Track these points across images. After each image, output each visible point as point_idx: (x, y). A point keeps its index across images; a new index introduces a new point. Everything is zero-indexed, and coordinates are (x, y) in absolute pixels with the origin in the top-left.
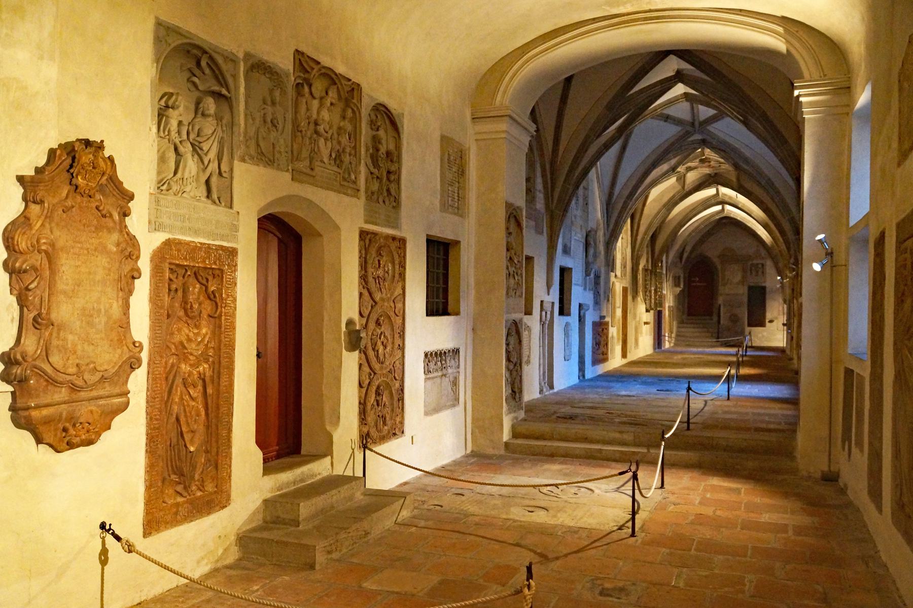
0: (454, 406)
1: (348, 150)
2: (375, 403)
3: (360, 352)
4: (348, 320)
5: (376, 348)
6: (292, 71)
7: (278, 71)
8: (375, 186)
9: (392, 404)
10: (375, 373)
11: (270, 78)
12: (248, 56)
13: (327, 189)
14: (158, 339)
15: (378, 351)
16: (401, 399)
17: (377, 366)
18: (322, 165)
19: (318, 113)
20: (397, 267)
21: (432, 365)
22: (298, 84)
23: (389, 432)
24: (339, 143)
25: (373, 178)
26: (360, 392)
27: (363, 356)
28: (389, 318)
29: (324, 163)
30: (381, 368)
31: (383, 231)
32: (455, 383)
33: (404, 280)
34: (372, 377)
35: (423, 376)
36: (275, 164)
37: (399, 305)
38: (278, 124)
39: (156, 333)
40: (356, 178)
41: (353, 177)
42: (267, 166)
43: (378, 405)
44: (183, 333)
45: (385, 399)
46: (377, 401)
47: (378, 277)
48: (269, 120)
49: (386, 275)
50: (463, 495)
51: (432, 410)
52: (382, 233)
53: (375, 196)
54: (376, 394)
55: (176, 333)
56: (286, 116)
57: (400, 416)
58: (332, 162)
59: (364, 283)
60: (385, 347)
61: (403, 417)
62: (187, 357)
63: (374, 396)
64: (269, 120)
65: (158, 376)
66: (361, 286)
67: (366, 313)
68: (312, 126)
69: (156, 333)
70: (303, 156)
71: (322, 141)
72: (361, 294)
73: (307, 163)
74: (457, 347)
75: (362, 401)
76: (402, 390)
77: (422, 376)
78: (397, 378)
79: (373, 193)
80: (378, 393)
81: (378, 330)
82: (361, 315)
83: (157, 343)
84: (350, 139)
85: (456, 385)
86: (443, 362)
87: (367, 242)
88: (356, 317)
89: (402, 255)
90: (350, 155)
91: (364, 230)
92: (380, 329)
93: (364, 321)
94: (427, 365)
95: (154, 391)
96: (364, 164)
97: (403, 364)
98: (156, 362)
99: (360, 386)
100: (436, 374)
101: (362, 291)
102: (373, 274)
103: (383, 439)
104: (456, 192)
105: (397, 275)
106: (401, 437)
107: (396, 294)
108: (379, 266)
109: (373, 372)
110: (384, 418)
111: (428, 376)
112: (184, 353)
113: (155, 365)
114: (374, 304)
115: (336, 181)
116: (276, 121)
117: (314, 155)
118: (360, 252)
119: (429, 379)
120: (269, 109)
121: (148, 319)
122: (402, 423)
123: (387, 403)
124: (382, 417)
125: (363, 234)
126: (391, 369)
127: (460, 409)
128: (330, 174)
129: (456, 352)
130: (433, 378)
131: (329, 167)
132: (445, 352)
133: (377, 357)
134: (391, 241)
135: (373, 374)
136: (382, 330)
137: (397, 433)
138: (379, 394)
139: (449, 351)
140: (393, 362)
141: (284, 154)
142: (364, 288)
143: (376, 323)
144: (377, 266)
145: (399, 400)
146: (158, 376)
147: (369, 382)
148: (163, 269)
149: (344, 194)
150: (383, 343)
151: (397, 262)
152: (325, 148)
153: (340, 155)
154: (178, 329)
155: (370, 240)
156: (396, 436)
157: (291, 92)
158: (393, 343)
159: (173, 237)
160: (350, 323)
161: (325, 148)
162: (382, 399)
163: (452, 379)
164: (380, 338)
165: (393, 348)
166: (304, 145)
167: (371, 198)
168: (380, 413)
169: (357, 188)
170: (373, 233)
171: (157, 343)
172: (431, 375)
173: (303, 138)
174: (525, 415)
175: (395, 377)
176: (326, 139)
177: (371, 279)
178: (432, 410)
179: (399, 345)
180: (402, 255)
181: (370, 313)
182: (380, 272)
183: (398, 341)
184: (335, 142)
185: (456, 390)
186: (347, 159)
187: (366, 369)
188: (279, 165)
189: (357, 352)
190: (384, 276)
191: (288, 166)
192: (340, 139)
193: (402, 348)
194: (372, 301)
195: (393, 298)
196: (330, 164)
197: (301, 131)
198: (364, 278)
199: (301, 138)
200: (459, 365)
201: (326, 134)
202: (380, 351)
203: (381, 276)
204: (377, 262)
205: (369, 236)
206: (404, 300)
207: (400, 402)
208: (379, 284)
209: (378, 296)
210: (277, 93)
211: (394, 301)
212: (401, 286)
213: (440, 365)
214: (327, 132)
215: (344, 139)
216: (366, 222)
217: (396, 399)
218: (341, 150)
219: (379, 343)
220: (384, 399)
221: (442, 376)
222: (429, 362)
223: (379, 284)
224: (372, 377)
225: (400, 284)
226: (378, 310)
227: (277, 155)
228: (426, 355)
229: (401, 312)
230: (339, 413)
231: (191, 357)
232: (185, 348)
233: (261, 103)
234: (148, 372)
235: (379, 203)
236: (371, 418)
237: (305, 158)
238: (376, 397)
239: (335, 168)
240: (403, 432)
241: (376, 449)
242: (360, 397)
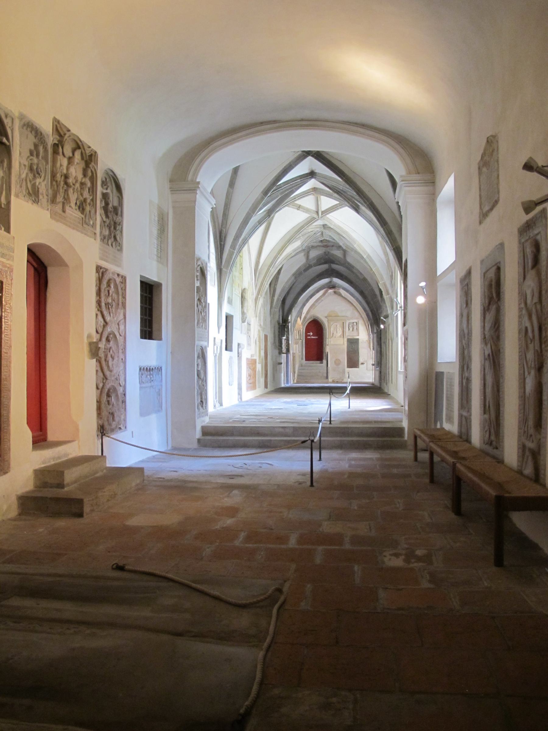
0: (159, 411)
1: (88, 201)
2: (107, 403)
3: (96, 361)
4: (88, 335)
6: (51, 134)
7: (43, 132)
8: (107, 233)
9: (118, 405)
10: (106, 379)
11: (35, 137)
12: (22, 117)
13: (74, 229)
15: (108, 362)
16: (124, 402)
17: (108, 373)
18: (70, 209)
19: (68, 169)
20: (120, 297)
21: (144, 376)
22: (55, 144)
23: (116, 427)
24: (82, 195)
25: (105, 226)
27: (98, 365)
28: (115, 336)
29: (72, 208)
30: (111, 375)
32: (159, 394)
35: (138, 385)
36: (39, 204)
37: (122, 327)
38: (41, 172)
40: (93, 224)
41: (91, 223)
42: (34, 204)
45: (113, 399)
46: (108, 401)
48: (35, 167)
50: (177, 472)
51: (144, 413)
54: (107, 396)
56: (47, 167)
57: (123, 415)
58: (77, 208)
59: (98, 307)
61: (125, 415)
63: (106, 397)
64: (35, 167)
66: (97, 309)
67: (100, 330)
68: (63, 177)
70: (58, 200)
71: (71, 191)
72: (97, 315)
73: (60, 205)
75: (98, 400)
76: (125, 395)
78: (121, 384)
79: (105, 238)
80: (108, 395)
82: (97, 332)
84: (89, 192)
85: (159, 395)
90: (90, 204)
91: (99, 265)
93: (98, 336)
94: (141, 377)
96: (99, 215)
97: (125, 375)
99: (97, 388)
105: (120, 304)
106: (125, 431)
110: (113, 414)
114: (105, 324)
115: (79, 223)
116: (39, 170)
117: (66, 199)
120: (35, 160)
122: (125, 420)
123: (115, 403)
124: (112, 413)
126: (117, 377)
127: (163, 413)
128: (76, 217)
131: (75, 211)
132: (152, 369)
133: (108, 366)
134: (116, 275)
135: (105, 380)
136: (110, 346)
137: (122, 428)
140: (118, 371)
141: (46, 197)
142: (98, 310)
144: (107, 295)
145: (123, 402)
147: (103, 386)
149: (86, 234)
150: (111, 355)
151: (120, 293)
152: (73, 197)
153: (82, 204)
156: (121, 430)
157: (50, 151)
158: (118, 357)
160: (89, 336)
161: (73, 197)
162: (111, 400)
163: (157, 391)
164: (110, 352)
165: (118, 360)
166: (59, 192)
167: (103, 240)
168: (110, 411)
169: (95, 232)
172: (144, 385)
173: (57, 186)
175: (119, 383)
176: (74, 189)
177: (103, 304)
178: (144, 413)
179: (122, 359)
182: (110, 300)
183: (121, 356)
184: (79, 193)
186: (88, 208)
187: (100, 374)
188: (41, 204)
189: (95, 360)
190: (112, 303)
191: (48, 206)
192: (82, 192)
193: (125, 363)
196: (76, 209)
197: (56, 181)
198: (99, 303)
199: (56, 186)
200: (162, 380)
201: (73, 186)
204: (107, 292)
205: (102, 270)
206: (125, 324)
207: (124, 403)
209: (108, 318)
210: (41, 149)
211: (118, 324)
213: (149, 379)
214: (74, 185)
216: (101, 259)
217: (121, 401)
219: (109, 356)
220: (113, 399)
222: (142, 375)
224: (104, 381)
225: (122, 311)
226: (109, 329)
227: (41, 197)
228: (140, 369)
229: (124, 333)
233: (29, 154)
235: (108, 245)
236: (105, 413)
237: (59, 202)
238: (107, 398)
239: (79, 214)
240: (126, 427)
242: (97, 396)
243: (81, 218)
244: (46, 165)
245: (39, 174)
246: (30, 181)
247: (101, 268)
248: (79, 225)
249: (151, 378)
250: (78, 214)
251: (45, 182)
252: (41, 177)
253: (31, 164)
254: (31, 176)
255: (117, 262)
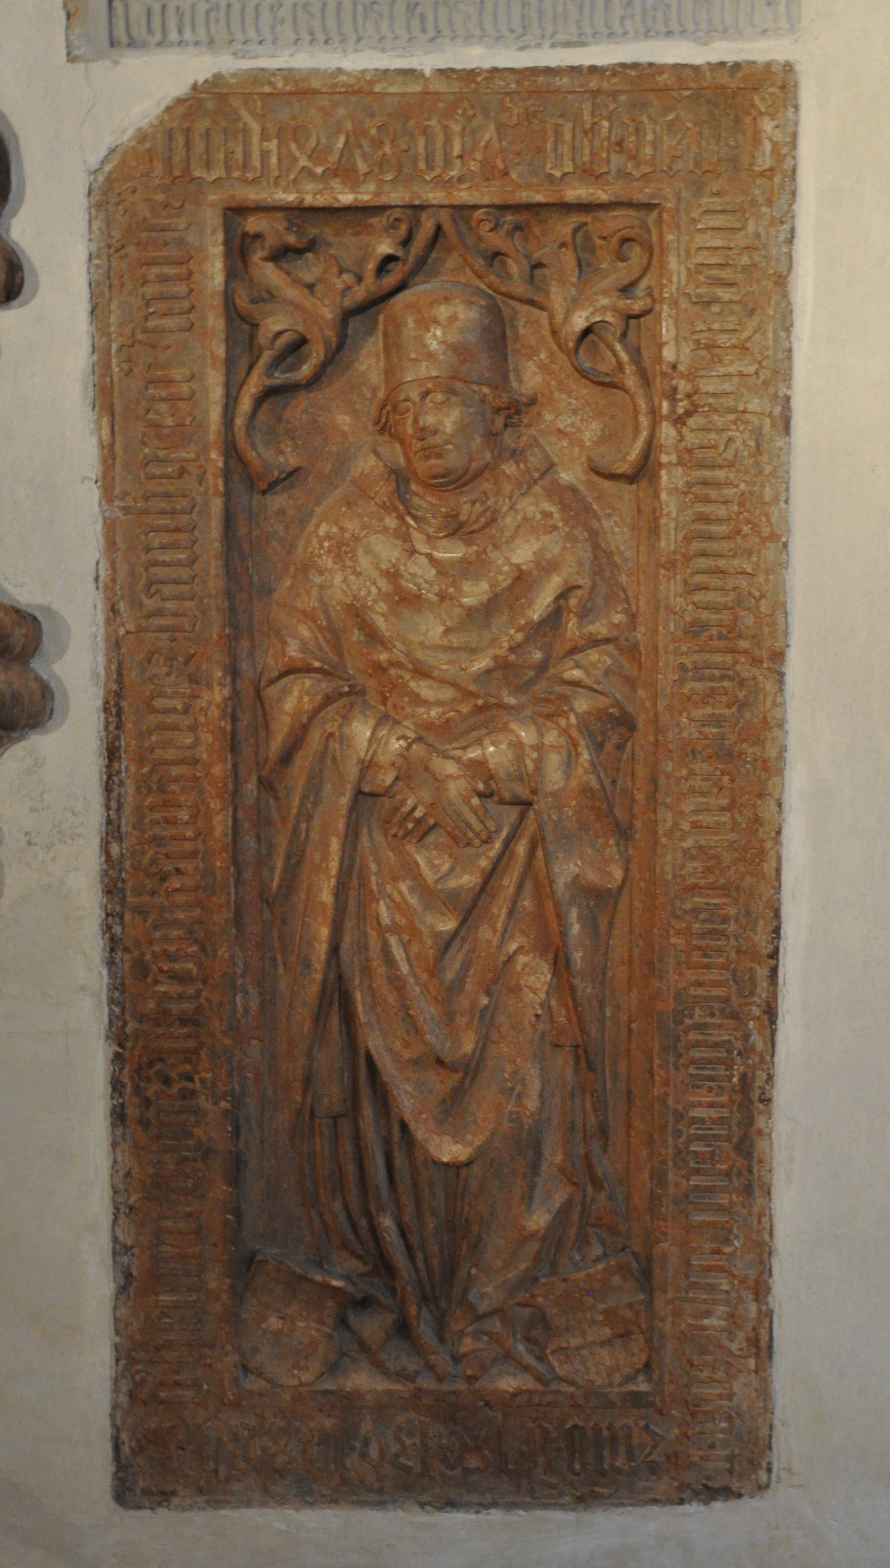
14: (167, 590)
39: (155, 563)
44: (364, 562)
55: (328, 562)
62: (397, 686)
65: (174, 771)
69: (155, 563)
83: (158, 613)
95: (157, 840)
98: (158, 703)
112: (380, 669)
113: (152, 720)
121: (93, 494)
146: (174, 771)
148: (181, 243)
154: (339, 545)
159: (246, 64)
171: (158, 613)
231: (425, 689)
232: (373, 636)
234: (112, 752)
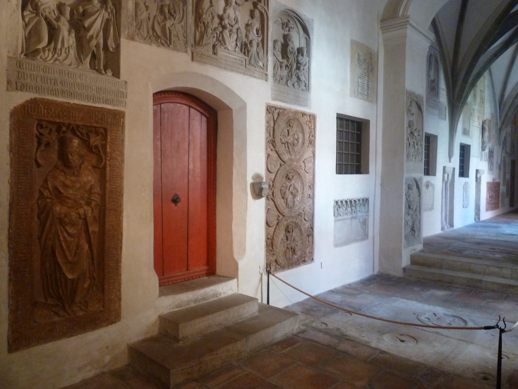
5: (286, 197)
8: (285, 73)
15: (287, 199)
25: (281, 67)
26: (267, 230)
31: (292, 108)
32: (365, 223)
33: (314, 146)
34: (280, 218)
41: (261, 64)
43: (287, 240)
47: (287, 143)
49: (296, 142)
52: (290, 109)
53: (285, 80)
60: (294, 196)
71: (226, 32)
74: (366, 197)
77: (332, 218)
78: (307, 220)
80: (287, 230)
81: (288, 183)
85: (365, 225)
86: (354, 208)
87: (276, 115)
88: (262, 172)
89: (313, 127)
92: (289, 182)
94: (338, 210)
100: (346, 217)
101: (271, 153)
102: (281, 140)
103: (283, 268)
104: (366, 83)
107: (306, 156)
108: (288, 135)
109: (282, 214)
111: (338, 218)
115: (242, 65)
118: (267, 122)
119: (339, 220)
125: (270, 109)
129: (366, 201)
130: (343, 220)
138: (289, 232)
139: (359, 200)
143: (286, 178)
144: (287, 134)
155: (278, 114)
158: (303, 193)
163: (361, 220)
170: (280, 108)
173: (205, 28)
174: (423, 247)
176: (231, 31)
180: (313, 127)
181: (278, 170)
183: (307, 191)
185: (366, 229)
186: (254, 49)
194: (280, 160)
195: (303, 159)
197: (204, 23)
200: (368, 210)
202: (289, 200)
203: (290, 142)
204: (286, 131)
208: (288, 148)
212: (311, 151)
215: (253, 35)
216: (274, 99)
217: (305, 235)
218: (248, 43)
221: (352, 218)
223: (288, 148)
230: (245, 247)
238: (286, 234)
239: (242, 55)
241: (276, 275)
243: (244, 60)
244: (184, 6)
245: (173, 16)
246: (159, 23)
247: (276, 108)
248: (241, 67)
249: (352, 210)
250: (239, 56)
251: (183, 23)
252: (175, 19)
253: (162, 6)
254: (160, 18)
255: (305, 103)
